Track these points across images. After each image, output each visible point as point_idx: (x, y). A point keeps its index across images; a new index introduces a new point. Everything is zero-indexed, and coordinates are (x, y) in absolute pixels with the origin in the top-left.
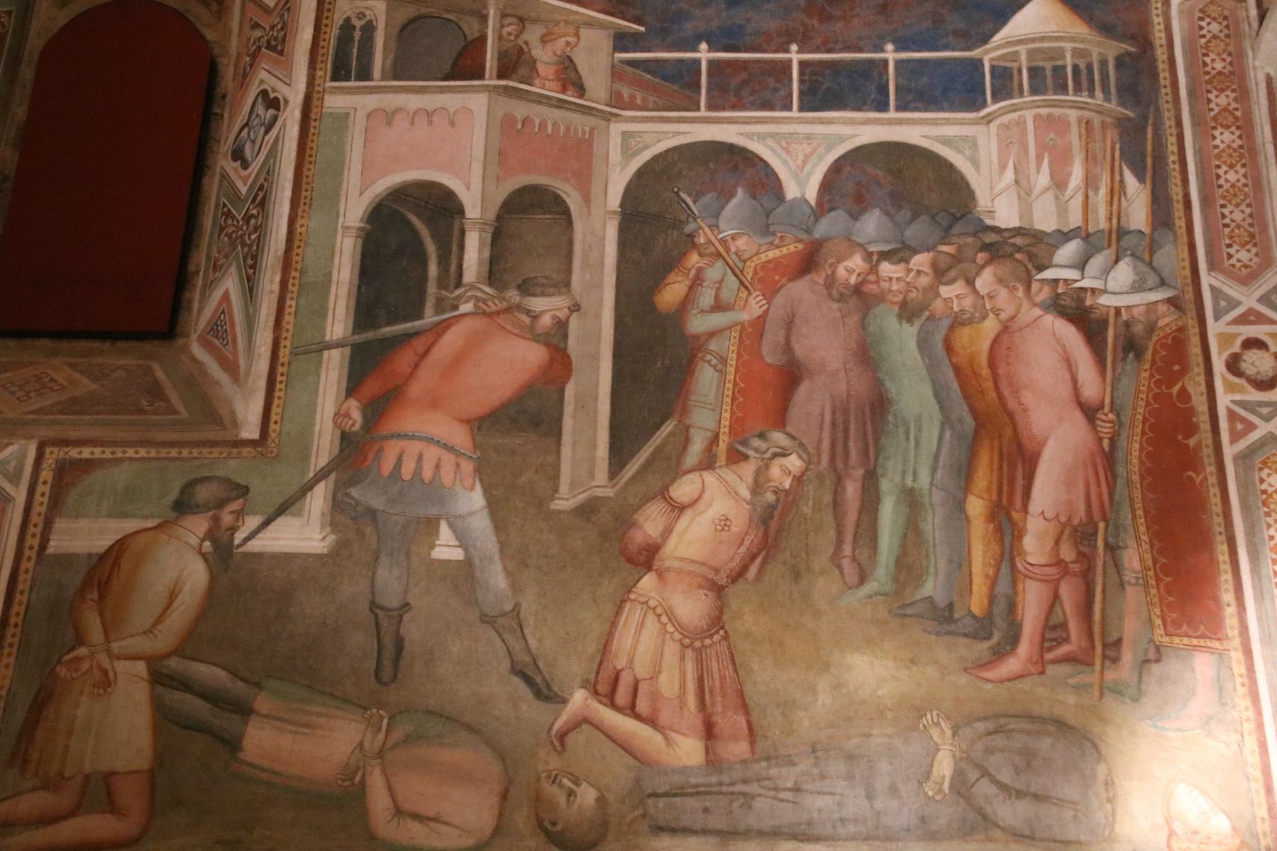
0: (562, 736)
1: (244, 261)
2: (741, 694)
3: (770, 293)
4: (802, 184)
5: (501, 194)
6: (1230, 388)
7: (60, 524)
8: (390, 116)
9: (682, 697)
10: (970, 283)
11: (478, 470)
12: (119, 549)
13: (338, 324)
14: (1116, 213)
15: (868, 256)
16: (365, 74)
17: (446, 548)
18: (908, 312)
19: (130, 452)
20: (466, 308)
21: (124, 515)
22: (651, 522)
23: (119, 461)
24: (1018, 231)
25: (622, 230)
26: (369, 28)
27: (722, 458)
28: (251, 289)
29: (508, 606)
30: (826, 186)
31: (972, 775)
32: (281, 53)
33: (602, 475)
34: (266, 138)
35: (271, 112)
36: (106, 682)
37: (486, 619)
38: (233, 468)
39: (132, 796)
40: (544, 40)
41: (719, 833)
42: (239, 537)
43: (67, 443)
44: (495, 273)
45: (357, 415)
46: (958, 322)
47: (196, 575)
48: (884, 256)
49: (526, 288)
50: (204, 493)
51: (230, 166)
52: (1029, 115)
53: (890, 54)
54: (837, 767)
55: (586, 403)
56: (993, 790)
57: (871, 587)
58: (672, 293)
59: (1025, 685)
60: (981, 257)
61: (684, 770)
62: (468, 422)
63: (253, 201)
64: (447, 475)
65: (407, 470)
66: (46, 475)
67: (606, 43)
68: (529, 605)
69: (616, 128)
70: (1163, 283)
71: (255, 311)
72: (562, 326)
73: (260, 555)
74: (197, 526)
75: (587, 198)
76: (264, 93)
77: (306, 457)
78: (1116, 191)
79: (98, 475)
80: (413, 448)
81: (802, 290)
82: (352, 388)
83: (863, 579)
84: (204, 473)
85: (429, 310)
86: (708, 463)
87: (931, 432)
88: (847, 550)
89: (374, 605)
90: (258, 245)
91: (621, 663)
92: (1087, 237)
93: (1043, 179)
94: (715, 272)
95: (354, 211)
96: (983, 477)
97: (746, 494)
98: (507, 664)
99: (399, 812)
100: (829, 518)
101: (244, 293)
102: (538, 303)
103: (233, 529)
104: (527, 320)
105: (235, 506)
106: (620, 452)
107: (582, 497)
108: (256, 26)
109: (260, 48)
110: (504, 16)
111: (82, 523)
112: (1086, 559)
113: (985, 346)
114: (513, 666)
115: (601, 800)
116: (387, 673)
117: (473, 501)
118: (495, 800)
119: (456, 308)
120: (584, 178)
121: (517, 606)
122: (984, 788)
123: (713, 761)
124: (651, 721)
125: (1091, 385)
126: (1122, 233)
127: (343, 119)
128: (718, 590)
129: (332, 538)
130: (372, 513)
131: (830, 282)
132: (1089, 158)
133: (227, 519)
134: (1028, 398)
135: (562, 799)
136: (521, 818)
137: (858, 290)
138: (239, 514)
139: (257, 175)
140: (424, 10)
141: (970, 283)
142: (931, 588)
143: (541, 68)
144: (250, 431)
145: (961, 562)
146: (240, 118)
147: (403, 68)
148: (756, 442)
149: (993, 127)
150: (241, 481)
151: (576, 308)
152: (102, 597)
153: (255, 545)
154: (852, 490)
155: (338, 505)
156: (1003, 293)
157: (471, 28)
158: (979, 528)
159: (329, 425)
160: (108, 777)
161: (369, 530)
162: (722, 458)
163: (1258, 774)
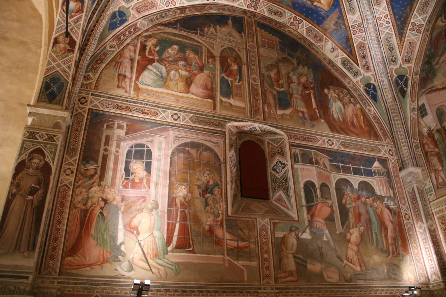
0: (344, 266)
1: (284, 190)
2: (363, 261)
3: (355, 202)
4: (356, 186)
5: (320, 184)
6: (405, 220)
7: (275, 232)
8: (303, 169)
9: (357, 261)
10: (377, 203)
11: (326, 227)
12: (284, 236)
13: (304, 203)
14: (390, 194)
15: (365, 198)
16: (298, 162)
17: (325, 239)
18: (371, 206)
19: (282, 221)
20: (320, 201)
21: (284, 232)
22: (348, 236)
23: (281, 223)
24: (380, 196)
25: (336, 191)
26: (297, 154)
27: (355, 227)
28: (288, 195)
29: (334, 248)
30: (358, 187)
31: (389, 272)
32: (283, 156)
33: (341, 229)
34: (283, 170)
35: (282, 165)
36: (288, 257)
37: (332, 250)
38: (296, 225)
39: (295, 274)
40: (320, 159)
41: (364, 280)
42: (299, 236)
43: (273, 219)
44: (322, 196)
45: (310, 217)
46: (376, 209)
47: (295, 241)
48: (367, 198)
49: (326, 199)
50: (293, 228)
51: (274, 173)
52: (378, 178)
53: (362, 167)
54: (375, 271)
55: (337, 218)
56: (391, 274)
57: (374, 246)
58: (344, 201)
59: (392, 260)
60: (377, 199)
61: (359, 271)
62: (323, 219)
63: (283, 179)
64: (323, 228)
65: (318, 226)
66: (272, 224)
67: (328, 161)
68: (337, 248)
69: (332, 175)
70: (396, 205)
71: (290, 199)
72: (332, 205)
73: (302, 239)
74: (293, 234)
75: (331, 185)
76: (280, 162)
77: (305, 223)
78: (389, 191)
79: (278, 225)
80: (318, 223)
81: (359, 202)
82: (308, 213)
83: (373, 245)
84: (292, 225)
85: (315, 202)
86: (353, 228)
87: (376, 224)
88: (371, 241)
89: (318, 247)
90: (287, 188)
91: (349, 256)
92: (387, 197)
93: (381, 188)
94: (348, 198)
95: (302, 185)
96: (383, 232)
97: (358, 232)
98: (336, 256)
99: (328, 277)
100: (368, 236)
101: (286, 196)
102: (328, 201)
103: (298, 234)
104: (327, 204)
105: (298, 231)
106: (343, 225)
107: (340, 232)
108: (273, 149)
109: (276, 153)
110: (314, 154)
111: (278, 232)
112: (395, 242)
113: (380, 212)
114: (337, 256)
115: (350, 275)
116: (322, 257)
117: (327, 231)
118: (338, 275)
119: (318, 201)
120: (330, 182)
121: (335, 248)
122: (390, 273)
123: (362, 270)
124: (354, 264)
125: (392, 219)
126: (391, 197)
127: (297, 169)
128: (358, 246)
129: (311, 236)
130: (315, 233)
131: (362, 201)
132: (386, 186)
133: (297, 233)
134: (386, 220)
135: (346, 275)
136: (342, 278)
137: (365, 203)
138: (299, 232)
139: (282, 175)
140: (304, 152)
141: (377, 203)
142: (380, 246)
143: (321, 164)
144: (297, 219)
145: (383, 243)
146: (273, 164)
147: (303, 162)
148: (358, 225)
149: (375, 180)
150: (298, 227)
151: (333, 203)
152: (284, 244)
153: (301, 237)
154: (369, 232)
155: (311, 232)
156: (380, 205)
157: (311, 156)
158: (384, 238)
159: (306, 219)
160: (291, 271)
161: (315, 235)
162: (355, 227)
163: (415, 271)
